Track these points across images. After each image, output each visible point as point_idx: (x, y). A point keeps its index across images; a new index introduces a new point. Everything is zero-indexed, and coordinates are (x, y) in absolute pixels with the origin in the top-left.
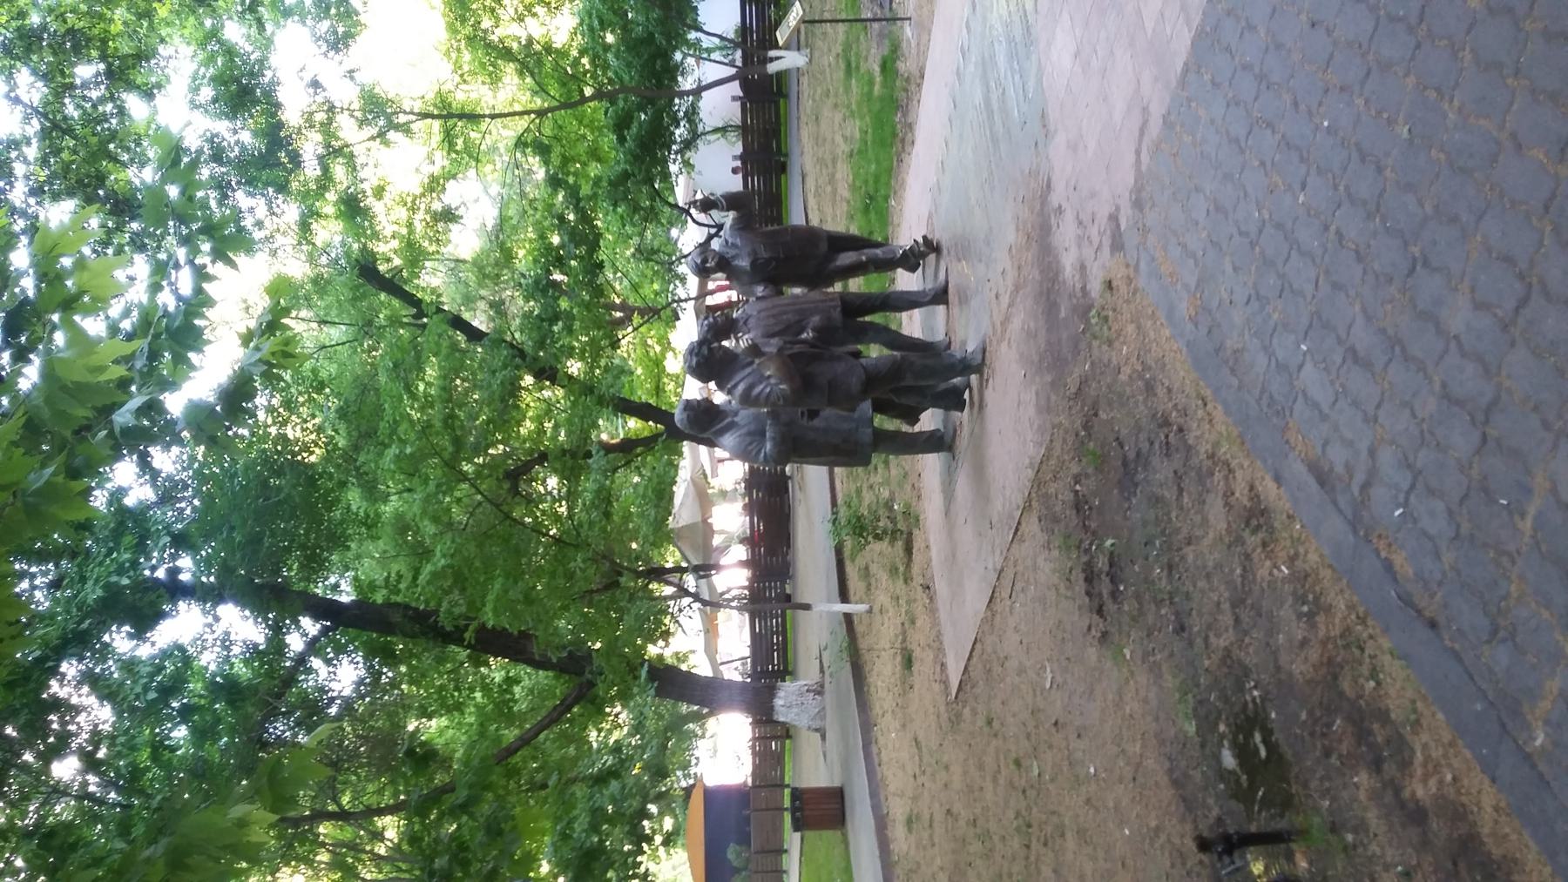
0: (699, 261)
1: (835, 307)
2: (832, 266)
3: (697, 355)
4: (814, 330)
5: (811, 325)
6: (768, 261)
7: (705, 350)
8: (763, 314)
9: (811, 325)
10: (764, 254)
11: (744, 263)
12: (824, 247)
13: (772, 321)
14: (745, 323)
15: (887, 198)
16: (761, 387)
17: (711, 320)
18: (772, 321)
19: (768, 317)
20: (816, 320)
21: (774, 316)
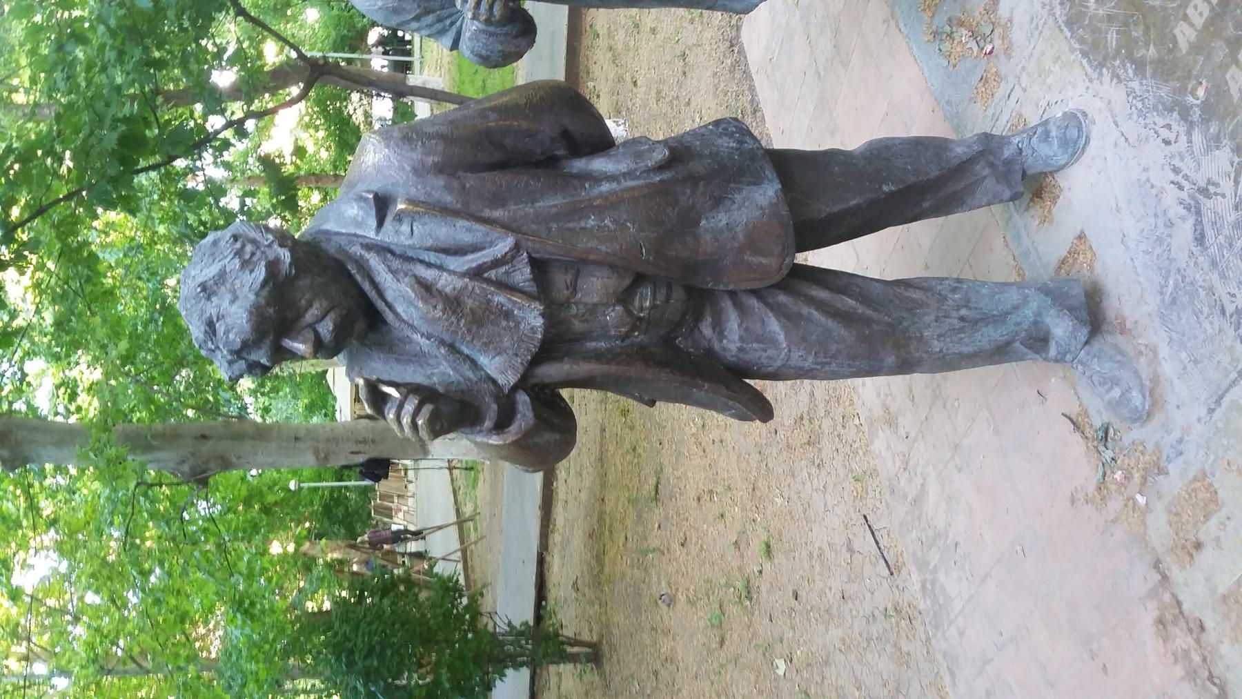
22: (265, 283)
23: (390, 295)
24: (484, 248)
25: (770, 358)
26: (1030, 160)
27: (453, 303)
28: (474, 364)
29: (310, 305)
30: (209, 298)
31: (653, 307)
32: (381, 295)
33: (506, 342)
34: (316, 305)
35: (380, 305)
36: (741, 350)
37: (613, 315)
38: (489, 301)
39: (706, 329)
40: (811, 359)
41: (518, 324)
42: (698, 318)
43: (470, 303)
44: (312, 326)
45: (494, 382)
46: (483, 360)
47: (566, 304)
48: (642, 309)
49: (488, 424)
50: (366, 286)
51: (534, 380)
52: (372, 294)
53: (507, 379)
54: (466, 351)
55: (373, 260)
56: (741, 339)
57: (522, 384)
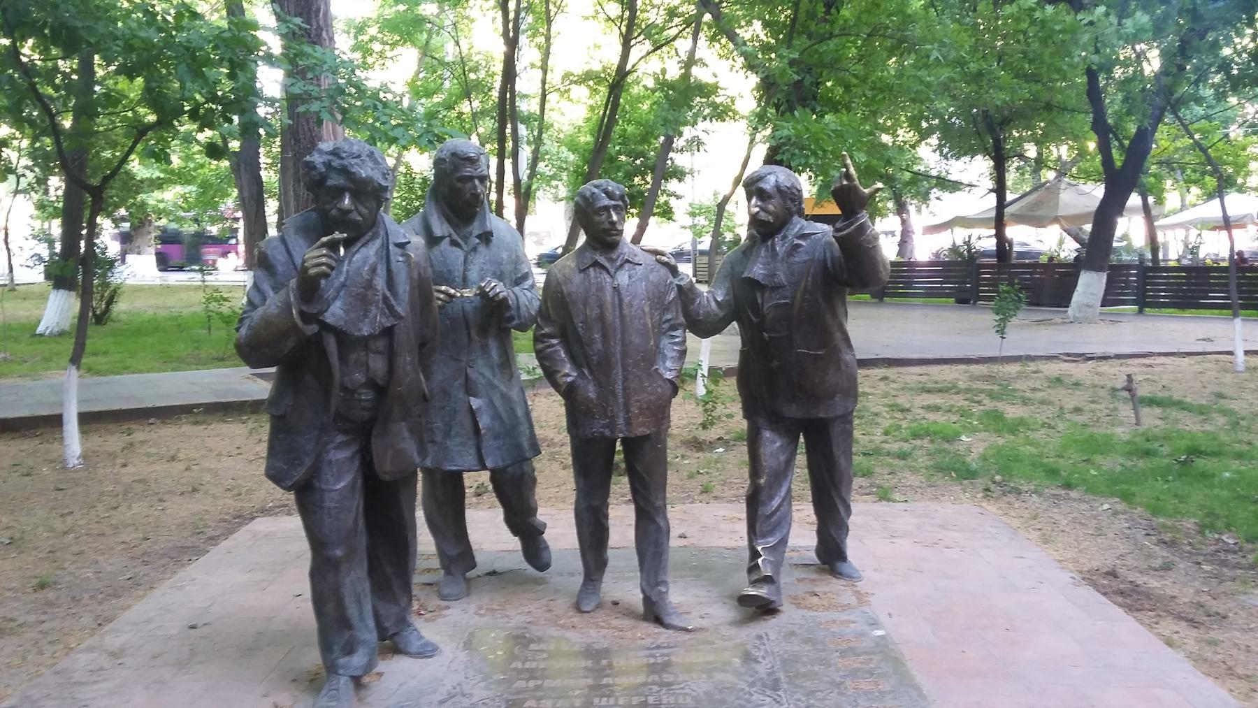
0: (762, 185)
1: (612, 426)
2: (761, 421)
3: (328, 165)
4: (571, 384)
5: (580, 381)
6: (756, 309)
7: (334, 181)
8: (608, 295)
9: (580, 381)
10: (768, 303)
11: (757, 271)
12: (793, 411)
13: (593, 312)
14: (596, 264)
15: (1126, 497)
16: (271, 293)
17: (606, 202)
18: (593, 312)
19: (601, 306)
20: (591, 392)
21: (601, 318)
22: (380, 185)
23: (364, 250)
24: (396, 300)
25: (327, 481)
26: (406, 634)
27: (369, 285)
28: (335, 298)
29: (366, 208)
30: (368, 155)
31: (360, 401)
32: (363, 245)
33: (353, 315)
34: (366, 211)
35: (359, 245)
36: (330, 462)
37: (359, 377)
38: (371, 305)
39: (340, 438)
40: (332, 505)
41: (361, 321)
42: (345, 432)
43: (370, 293)
44: (356, 209)
45: (326, 311)
46: (338, 303)
47: (366, 348)
48: (360, 394)
49: (305, 308)
50: (367, 237)
51: (324, 334)
52: (363, 241)
53: (329, 318)
54: (342, 293)
55: (378, 242)
56: (338, 460)
57: (325, 326)
